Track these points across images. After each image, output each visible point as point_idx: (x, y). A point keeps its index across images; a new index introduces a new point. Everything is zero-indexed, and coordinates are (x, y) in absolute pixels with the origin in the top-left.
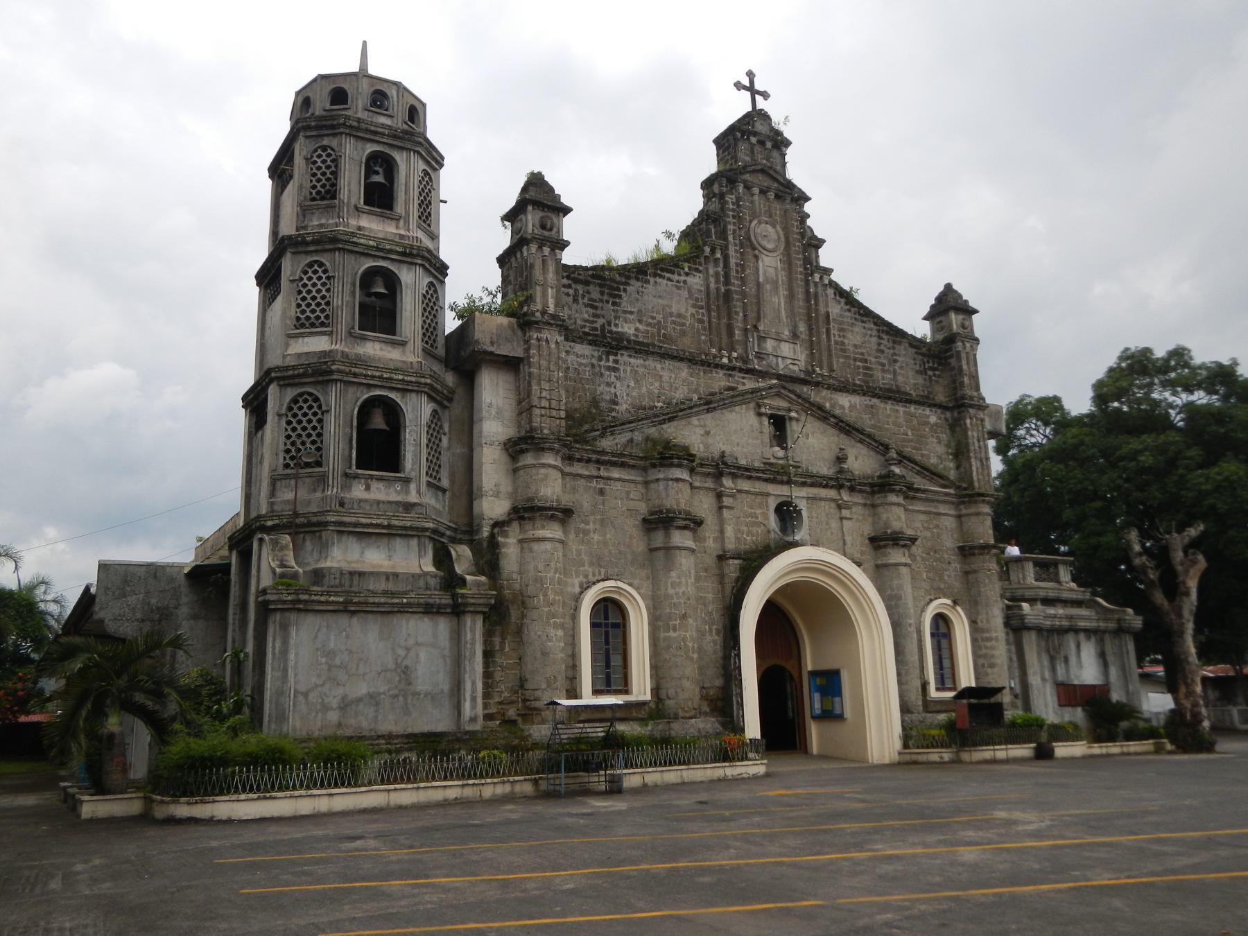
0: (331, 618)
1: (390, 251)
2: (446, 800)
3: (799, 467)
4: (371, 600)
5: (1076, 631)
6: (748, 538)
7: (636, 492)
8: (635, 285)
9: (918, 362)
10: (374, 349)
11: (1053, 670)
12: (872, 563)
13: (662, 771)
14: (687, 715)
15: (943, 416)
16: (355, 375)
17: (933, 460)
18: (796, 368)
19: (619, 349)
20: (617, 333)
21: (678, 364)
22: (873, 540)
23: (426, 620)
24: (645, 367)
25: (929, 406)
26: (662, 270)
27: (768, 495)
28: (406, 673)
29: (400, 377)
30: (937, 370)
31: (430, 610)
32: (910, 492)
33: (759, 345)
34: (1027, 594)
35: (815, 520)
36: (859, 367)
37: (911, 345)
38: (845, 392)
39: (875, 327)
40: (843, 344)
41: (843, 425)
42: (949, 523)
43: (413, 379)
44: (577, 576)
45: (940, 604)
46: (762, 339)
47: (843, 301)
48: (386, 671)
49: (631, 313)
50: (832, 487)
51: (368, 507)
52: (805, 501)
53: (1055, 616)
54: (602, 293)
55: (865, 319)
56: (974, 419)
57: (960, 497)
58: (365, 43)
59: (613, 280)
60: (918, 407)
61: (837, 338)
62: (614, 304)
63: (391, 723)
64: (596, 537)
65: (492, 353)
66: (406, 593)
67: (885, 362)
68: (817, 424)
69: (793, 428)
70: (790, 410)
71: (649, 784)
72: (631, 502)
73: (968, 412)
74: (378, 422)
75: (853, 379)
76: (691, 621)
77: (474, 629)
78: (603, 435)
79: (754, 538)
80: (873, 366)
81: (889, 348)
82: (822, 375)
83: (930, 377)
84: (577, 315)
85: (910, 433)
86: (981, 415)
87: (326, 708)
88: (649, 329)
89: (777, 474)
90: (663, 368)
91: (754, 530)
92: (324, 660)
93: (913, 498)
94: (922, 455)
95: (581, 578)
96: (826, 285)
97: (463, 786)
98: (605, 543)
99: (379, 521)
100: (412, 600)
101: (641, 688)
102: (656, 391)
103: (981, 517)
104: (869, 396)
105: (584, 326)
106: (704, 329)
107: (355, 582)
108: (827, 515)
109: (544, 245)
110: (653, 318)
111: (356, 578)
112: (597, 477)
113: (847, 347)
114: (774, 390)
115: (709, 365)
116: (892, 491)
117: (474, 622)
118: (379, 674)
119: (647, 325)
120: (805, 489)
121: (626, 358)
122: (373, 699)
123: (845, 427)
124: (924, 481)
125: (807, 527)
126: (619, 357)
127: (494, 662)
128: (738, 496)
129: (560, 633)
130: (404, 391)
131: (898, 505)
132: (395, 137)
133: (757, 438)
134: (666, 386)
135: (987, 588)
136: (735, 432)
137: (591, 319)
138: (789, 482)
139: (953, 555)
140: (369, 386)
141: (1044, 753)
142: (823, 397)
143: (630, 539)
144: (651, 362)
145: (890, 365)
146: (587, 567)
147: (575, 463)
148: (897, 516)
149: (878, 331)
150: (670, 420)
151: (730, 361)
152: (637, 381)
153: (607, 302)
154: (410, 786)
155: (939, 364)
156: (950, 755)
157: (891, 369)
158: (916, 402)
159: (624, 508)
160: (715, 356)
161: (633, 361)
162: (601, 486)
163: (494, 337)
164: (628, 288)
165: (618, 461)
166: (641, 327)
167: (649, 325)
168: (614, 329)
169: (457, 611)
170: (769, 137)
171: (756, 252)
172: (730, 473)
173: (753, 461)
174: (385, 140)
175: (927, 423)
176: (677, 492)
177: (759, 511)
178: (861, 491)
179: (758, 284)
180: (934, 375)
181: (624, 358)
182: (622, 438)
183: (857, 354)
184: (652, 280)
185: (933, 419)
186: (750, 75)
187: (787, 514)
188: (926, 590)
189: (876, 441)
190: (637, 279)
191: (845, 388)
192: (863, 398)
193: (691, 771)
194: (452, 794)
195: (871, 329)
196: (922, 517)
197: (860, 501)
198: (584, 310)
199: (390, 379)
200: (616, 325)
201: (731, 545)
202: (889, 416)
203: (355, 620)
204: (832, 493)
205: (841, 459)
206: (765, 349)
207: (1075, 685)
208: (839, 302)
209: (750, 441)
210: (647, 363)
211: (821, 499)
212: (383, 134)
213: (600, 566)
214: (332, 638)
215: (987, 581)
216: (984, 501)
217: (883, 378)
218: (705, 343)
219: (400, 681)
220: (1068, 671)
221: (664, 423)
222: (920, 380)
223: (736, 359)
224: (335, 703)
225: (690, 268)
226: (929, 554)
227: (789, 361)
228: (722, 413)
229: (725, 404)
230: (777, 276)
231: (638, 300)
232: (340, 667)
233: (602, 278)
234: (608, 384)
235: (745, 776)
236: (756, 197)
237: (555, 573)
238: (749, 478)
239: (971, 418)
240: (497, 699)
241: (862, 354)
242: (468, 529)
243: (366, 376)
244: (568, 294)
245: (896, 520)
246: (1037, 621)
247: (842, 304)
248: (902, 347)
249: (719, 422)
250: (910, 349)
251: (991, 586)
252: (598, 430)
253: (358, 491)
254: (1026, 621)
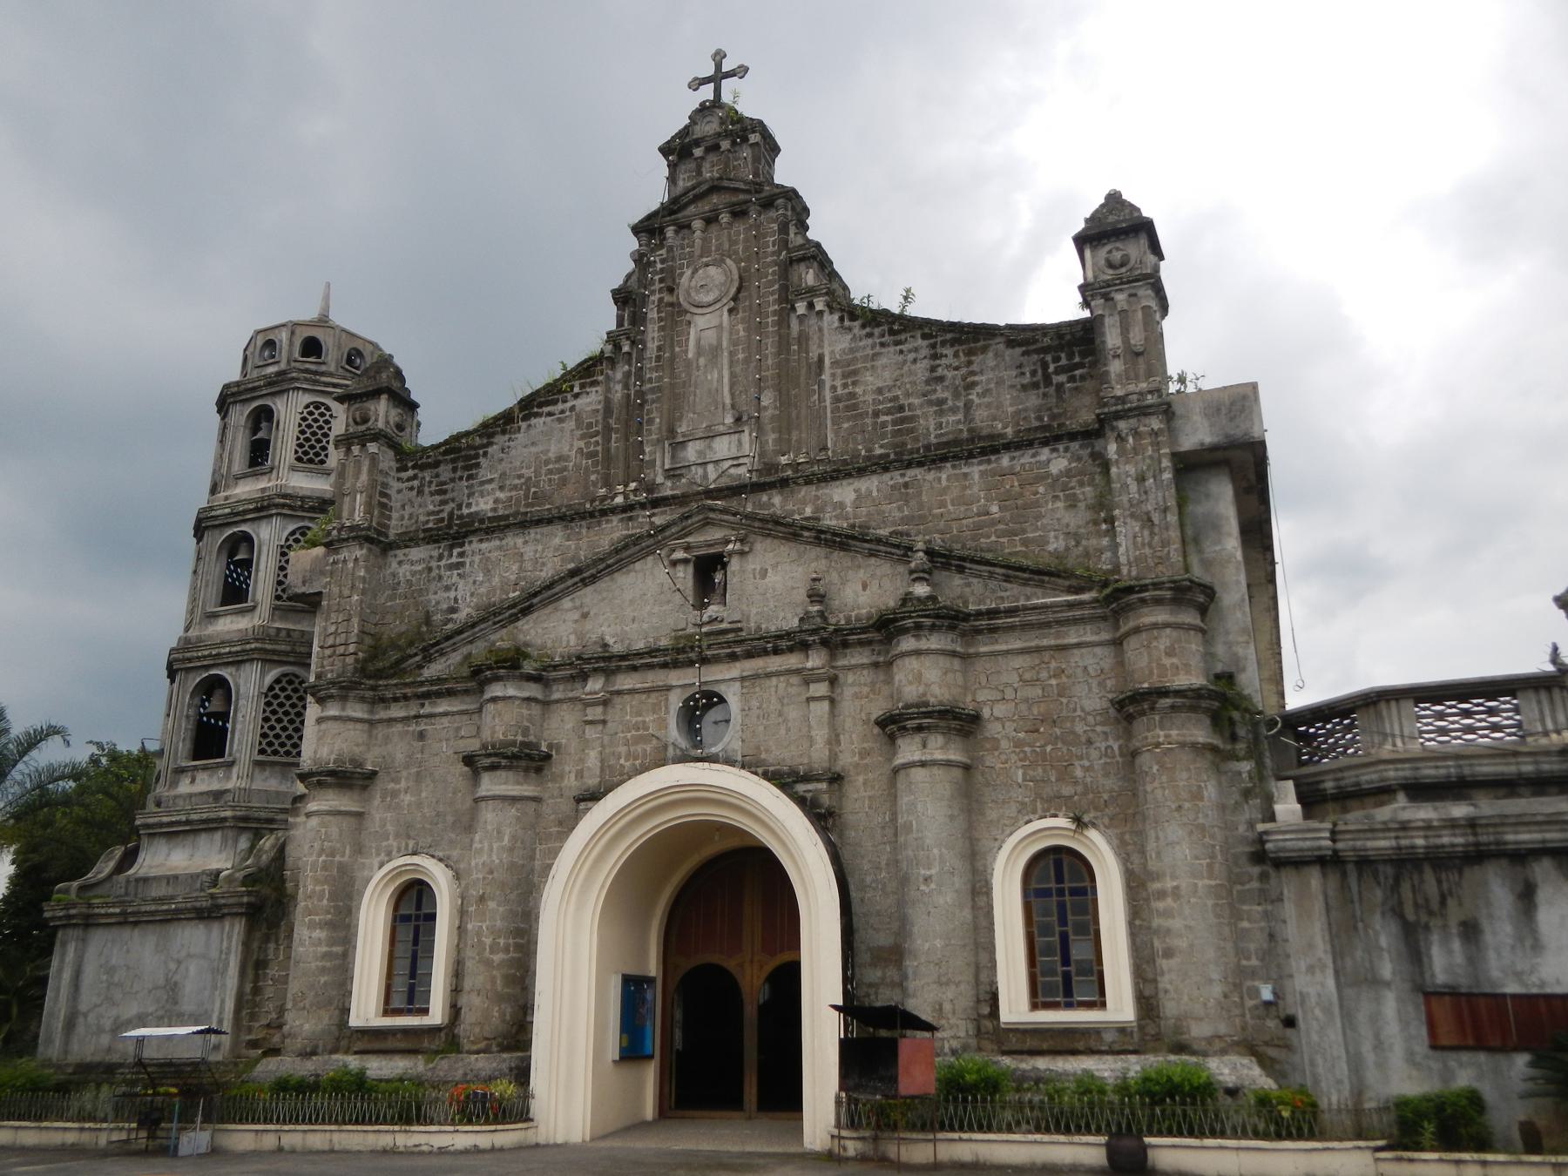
0: (115, 931)
1: (245, 512)
2: (63, 1145)
3: (741, 630)
4: (143, 909)
5: (1520, 857)
6: (628, 764)
8: (500, 440)
9: (1027, 370)
10: (231, 625)
11: (1415, 954)
12: (887, 769)
13: (305, 1131)
14: (475, 1048)
15: (1085, 453)
16: (190, 660)
17: (1056, 544)
18: (742, 471)
19: (465, 537)
20: (470, 515)
21: (546, 529)
22: (882, 723)
23: (201, 927)
24: (500, 548)
25: (1045, 443)
26: (540, 405)
27: (669, 688)
29: (227, 650)
30: (1080, 365)
32: (952, 619)
33: (673, 457)
34: (1364, 778)
35: (755, 712)
36: (884, 424)
37: (1011, 344)
38: (844, 478)
39: (926, 343)
40: (852, 395)
41: (829, 537)
42: (1096, 660)
43: (238, 648)
44: (378, 855)
45: (1054, 828)
46: (678, 446)
47: (857, 324)
48: (156, 988)
49: (491, 481)
50: (791, 650)
51: (181, 803)
52: (738, 684)
53: (1405, 827)
54: (454, 470)
55: (903, 337)
56: (1131, 440)
57: (1108, 600)
58: (328, 285)
59: (470, 447)
60: (1017, 454)
61: (840, 391)
62: (468, 479)
64: (407, 798)
65: (304, 594)
66: (172, 897)
67: (946, 395)
68: (785, 550)
70: (728, 542)
71: (287, 1147)
72: (460, 742)
73: (1113, 429)
75: (869, 450)
76: (492, 905)
78: (428, 659)
79: (637, 762)
80: (918, 412)
81: (956, 369)
82: (795, 466)
83: (1060, 386)
84: (421, 510)
85: (994, 509)
86: (1156, 423)
87: (100, 1030)
88: (514, 493)
89: (682, 654)
90: (526, 542)
91: (639, 748)
92: (105, 977)
93: (978, 631)
94: (1025, 542)
95: (383, 857)
96: (820, 313)
97: (82, 1129)
98: (419, 805)
99: (178, 818)
100: (180, 905)
102: (513, 577)
103: (1144, 635)
104: (897, 469)
105: (427, 522)
106: (596, 464)
107: (140, 890)
108: (781, 700)
109: (352, 444)
110: (520, 477)
111: (141, 884)
112: (417, 717)
113: (861, 399)
114: (695, 519)
115: (592, 515)
116: (904, 631)
117: (232, 926)
118: (150, 992)
119: (510, 490)
120: (738, 664)
121: (475, 546)
124: (1028, 590)
125: (738, 728)
126: (467, 547)
127: (265, 975)
128: (617, 700)
129: (318, 934)
130: (238, 664)
131: (918, 653)
132: (270, 384)
133: (669, 602)
134: (528, 566)
135: (1156, 784)
136: (632, 602)
137: (437, 509)
138: (705, 661)
139: (1102, 724)
140: (207, 667)
142: (799, 505)
143: (454, 793)
145: (956, 395)
146: (390, 842)
147: (393, 705)
149: (933, 346)
150: (526, 611)
151: (626, 497)
152: (487, 572)
153: (461, 478)
154: (33, 1125)
155: (1083, 355)
156: (859, 1145)
157: (961, 404)
158: (1008, 447)
159: (450, 752)
160: (604, 499)
161: (484, 546)
162: (423, 727)
163: (308, 574)
164: (490, 450)
165: (441, 690)
166: (502, 495)
167: (515, 488)
168: (465, 511)
170: (719, 134)
171: (688, 317)
172: (595, 670)
173: (657, 639)
174: (264, 392)
175: (1048, 475)
176: (494, 718)
177: (649, 718)
178: (861, 643)
179: (688, 363)
180: (1072, 379)
181: (474, 546)
183: (880, 403)
184: (524, 425)
185: (1059, 464)
186: (719, 57)
188: (1023, 804)
189: (897, 546)
190: (504, 432)
192: (886, 476)
193: (344, 1135)
194: (71, 1138)
195: (916, 350)
196: (1019, 662)
197: (865, 661)
198: (429, 499)
199: (218, 654)
200: (469, 505)
202: (945, 491)
203: (136, 931)
204: (792, 661)
206: (684, 459)
207: (1504, 996)
208: (850, 329)
209: (656, 609)
210: (504, 542)
211: (769, 675)
212: (259, 387)
213: (409, 837)
214: (115, 951)
215: (1155, 768)
216: (1143, 601)
217: (940, 426)
218: (595, 484)
219: (167, 1001)
220: (1475, 957)
221: (518, 619)
222: (1033, 400)
223: (636, 490)
224: (107, 1024)
225: (582, 386)
226: (1037, 731)
227: (726, 464)
228: (612, 580)
229: (609, 566)
230: (720, 339)
231: (502, 460)
232: (117, 985)
233: (459, 450)
234: (447, 588)
235: (425, 1148)
236: (698, 233)
237: (319, 855)
238: (635, 668)
239: (1120, 439)
240: (264, 1022)
241: (896, 398)
243: (198, 658)
244: (412, 489)
245: (911, 683)
246: (1308, 844)
247: (856, 331)
248: (991, 354)
249: (605, 595)
250: (1009, 352)
251: (1164, 778)
252: (416, 655)
254: (1269, 846)
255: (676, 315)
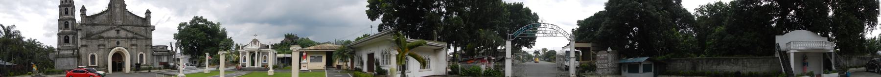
7: (97, 42)
10: (66, 31)
28: (69, 64)
31: (71, 57)
32: (137, 38)
63: (68, 68)
69: (120, 32)
74: (67, 38)
77: (76, 59)
78: (92, 36)
89: (117, 38)
101: (97, 65)
122: (66, 66)
123: (128, 31)
141: (149, 72)
142: (125, 27)
144: (100, 26)
148: (134, 42)
165: (94, 39)
169: (74, 57)
182: (95, 36)
187: (118, 43)
191: (128, 25)
201: (109, 47)
205: (127, 35)
242: (77, 49)
253: (65, 46)
255: (115, 8)
